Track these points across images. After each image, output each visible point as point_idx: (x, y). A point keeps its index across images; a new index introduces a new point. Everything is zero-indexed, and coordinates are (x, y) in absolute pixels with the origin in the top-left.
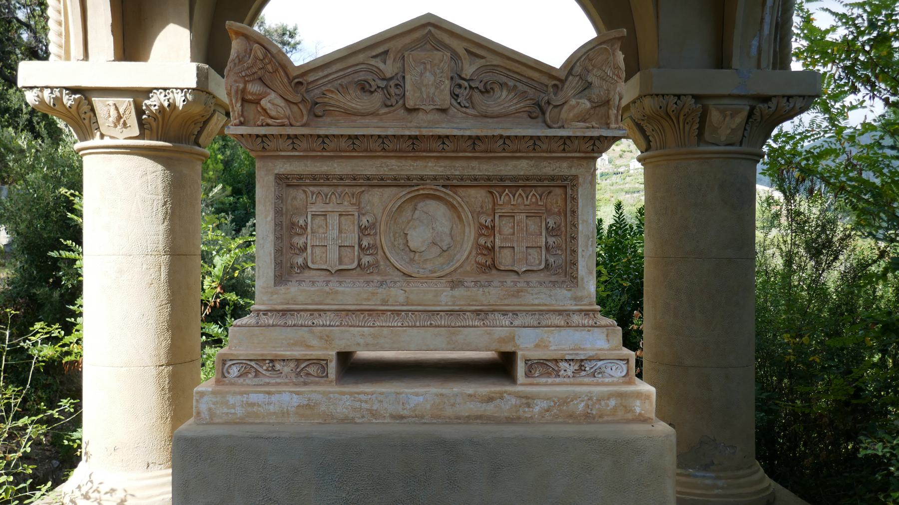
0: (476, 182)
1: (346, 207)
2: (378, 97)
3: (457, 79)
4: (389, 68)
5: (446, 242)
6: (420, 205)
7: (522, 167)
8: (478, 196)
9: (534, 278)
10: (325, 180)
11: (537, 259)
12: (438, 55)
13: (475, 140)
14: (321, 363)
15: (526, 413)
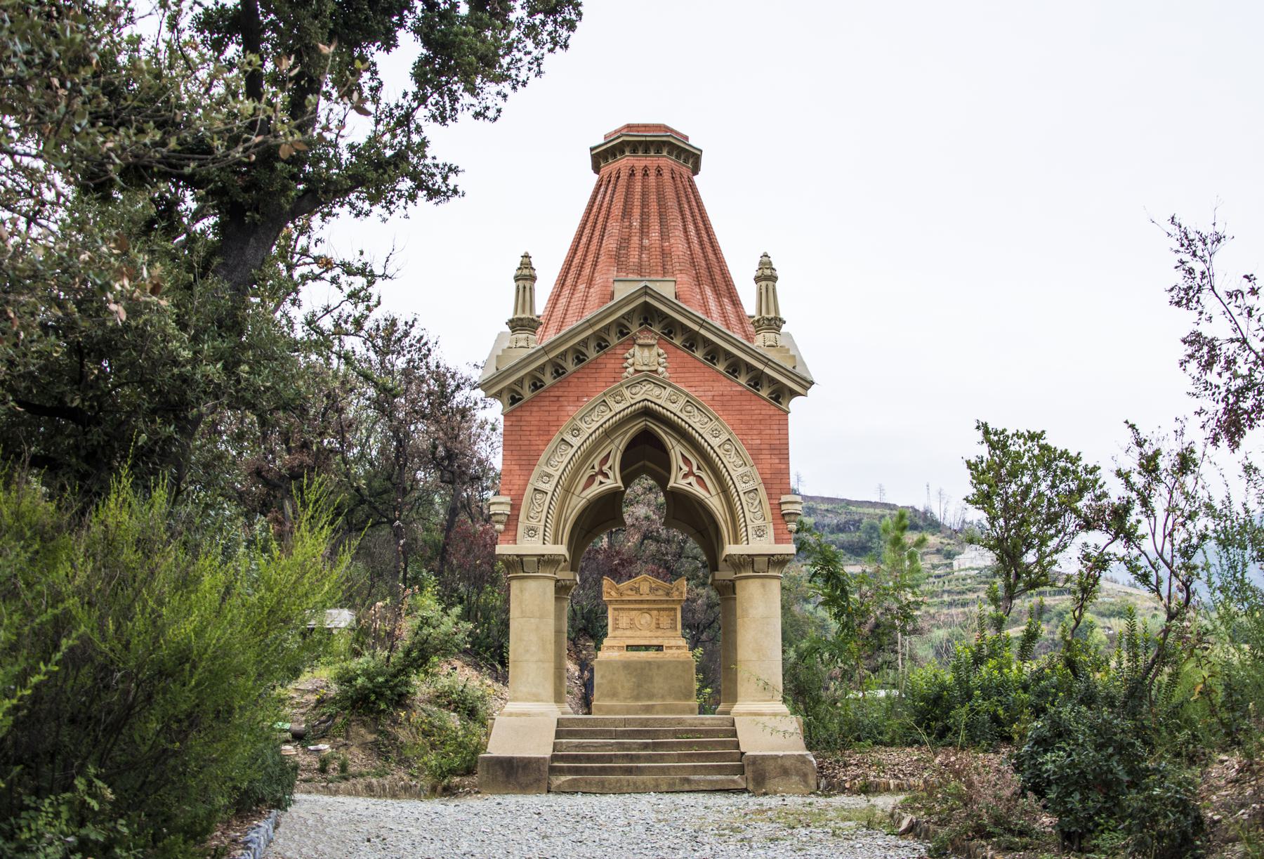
0: (655, 609)
3: (651, 588)
4: (637, 586)
7: (665, 606)
8: (655, 613)
10: (621, 609)
11: (669, 626)
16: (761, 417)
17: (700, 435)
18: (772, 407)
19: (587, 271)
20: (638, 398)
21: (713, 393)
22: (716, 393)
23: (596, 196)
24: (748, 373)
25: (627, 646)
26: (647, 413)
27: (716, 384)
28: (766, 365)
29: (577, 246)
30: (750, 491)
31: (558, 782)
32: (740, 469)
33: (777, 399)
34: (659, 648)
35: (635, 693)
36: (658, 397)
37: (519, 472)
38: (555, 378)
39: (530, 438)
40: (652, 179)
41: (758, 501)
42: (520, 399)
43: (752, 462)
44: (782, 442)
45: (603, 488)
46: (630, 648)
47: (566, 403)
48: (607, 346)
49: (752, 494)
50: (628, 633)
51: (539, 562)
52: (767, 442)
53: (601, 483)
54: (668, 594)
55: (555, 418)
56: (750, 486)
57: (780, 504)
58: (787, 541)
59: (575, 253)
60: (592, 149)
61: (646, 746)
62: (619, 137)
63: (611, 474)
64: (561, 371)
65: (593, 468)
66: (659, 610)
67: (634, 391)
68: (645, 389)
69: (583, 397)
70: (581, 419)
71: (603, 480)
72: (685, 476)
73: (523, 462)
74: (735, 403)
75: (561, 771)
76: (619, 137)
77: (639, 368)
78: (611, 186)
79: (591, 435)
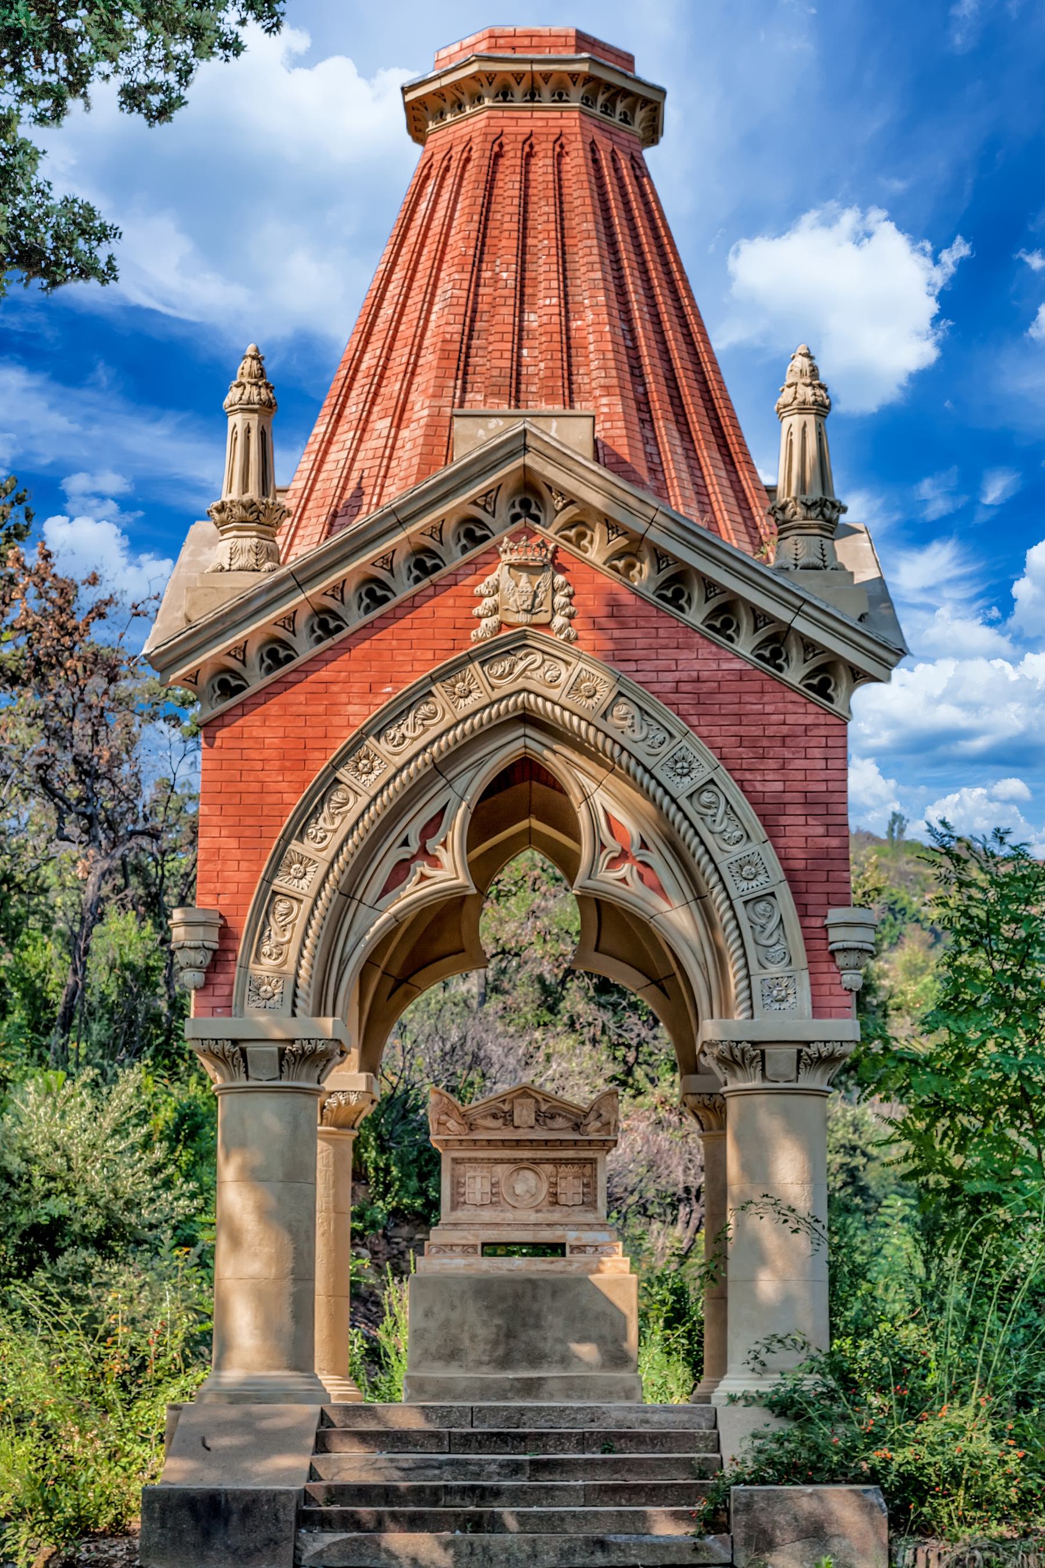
0: (548, 1161)
1: (485, 1174)
2: (501, 1121)
3: (538, 1113)
4: (506, 1107)
5: (533, 1191)
6: (522, 1172)
7: (570, 1154)
8: (549, 1168)
9: (576, 1208)
11: (578, 1199)
12: (530, 1100)
13: (546, 1142)
14: (474, 1246)
15: (569, 1269)
16: (785, 730)
17: (646, 770)
18: (811, 708)
19: (393, 387)
20: (507, 686)
21: (677, 675)
22: (684, 676)
23: (417, 204)
24: (756, 629)
25: (484, 1245)
26: (527, 718)
27: (684, 654)
28: (798, 611)
29: (373, 324)
30: (759, 899)
31: (318, 1546)
32: (735, 849)
33: (822, 690)
34: (557, 1249)
35: (500, 1351)
36: (553, 683)
37: (238, 854)
38: (319, 640)
39: (262, 775)
40: (542, 167)
41: (775, 920)
42: (240, 689)
43: (763, 835)
44: (832, 786)
45: (426, 889)
46: (490, 1249)
47: (344, 698)
48: (436, 568)
49: (762, 906)
50: (487, 1215)
51: (282, 1053)
52: (800, 786)
53: (423, 877)
54: (577, 1127)
55: (320, 732)
56: (756, 887)
57: (825, 928)
58: (840, 1012)
59: (367, 342)
60: (405, 91)
61: (515, 1468)
62: (468, 63)
63: (445, 857)
64: (332, 624)
65: (406, 843)
66: (556, 1162)
67: (498, 669)
68: (522, 665)
69: (383, 683)
70: (378, 737)
71: (428, 871)
72: (614, 863)
73: (248, 832)
74: (727, 698)
75: (325, 1522)
76: (468, 63)
77: (512, 619)
78: (449, 181)
79: (400, 770)
